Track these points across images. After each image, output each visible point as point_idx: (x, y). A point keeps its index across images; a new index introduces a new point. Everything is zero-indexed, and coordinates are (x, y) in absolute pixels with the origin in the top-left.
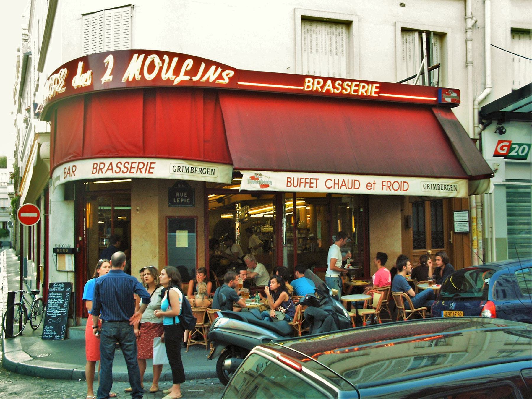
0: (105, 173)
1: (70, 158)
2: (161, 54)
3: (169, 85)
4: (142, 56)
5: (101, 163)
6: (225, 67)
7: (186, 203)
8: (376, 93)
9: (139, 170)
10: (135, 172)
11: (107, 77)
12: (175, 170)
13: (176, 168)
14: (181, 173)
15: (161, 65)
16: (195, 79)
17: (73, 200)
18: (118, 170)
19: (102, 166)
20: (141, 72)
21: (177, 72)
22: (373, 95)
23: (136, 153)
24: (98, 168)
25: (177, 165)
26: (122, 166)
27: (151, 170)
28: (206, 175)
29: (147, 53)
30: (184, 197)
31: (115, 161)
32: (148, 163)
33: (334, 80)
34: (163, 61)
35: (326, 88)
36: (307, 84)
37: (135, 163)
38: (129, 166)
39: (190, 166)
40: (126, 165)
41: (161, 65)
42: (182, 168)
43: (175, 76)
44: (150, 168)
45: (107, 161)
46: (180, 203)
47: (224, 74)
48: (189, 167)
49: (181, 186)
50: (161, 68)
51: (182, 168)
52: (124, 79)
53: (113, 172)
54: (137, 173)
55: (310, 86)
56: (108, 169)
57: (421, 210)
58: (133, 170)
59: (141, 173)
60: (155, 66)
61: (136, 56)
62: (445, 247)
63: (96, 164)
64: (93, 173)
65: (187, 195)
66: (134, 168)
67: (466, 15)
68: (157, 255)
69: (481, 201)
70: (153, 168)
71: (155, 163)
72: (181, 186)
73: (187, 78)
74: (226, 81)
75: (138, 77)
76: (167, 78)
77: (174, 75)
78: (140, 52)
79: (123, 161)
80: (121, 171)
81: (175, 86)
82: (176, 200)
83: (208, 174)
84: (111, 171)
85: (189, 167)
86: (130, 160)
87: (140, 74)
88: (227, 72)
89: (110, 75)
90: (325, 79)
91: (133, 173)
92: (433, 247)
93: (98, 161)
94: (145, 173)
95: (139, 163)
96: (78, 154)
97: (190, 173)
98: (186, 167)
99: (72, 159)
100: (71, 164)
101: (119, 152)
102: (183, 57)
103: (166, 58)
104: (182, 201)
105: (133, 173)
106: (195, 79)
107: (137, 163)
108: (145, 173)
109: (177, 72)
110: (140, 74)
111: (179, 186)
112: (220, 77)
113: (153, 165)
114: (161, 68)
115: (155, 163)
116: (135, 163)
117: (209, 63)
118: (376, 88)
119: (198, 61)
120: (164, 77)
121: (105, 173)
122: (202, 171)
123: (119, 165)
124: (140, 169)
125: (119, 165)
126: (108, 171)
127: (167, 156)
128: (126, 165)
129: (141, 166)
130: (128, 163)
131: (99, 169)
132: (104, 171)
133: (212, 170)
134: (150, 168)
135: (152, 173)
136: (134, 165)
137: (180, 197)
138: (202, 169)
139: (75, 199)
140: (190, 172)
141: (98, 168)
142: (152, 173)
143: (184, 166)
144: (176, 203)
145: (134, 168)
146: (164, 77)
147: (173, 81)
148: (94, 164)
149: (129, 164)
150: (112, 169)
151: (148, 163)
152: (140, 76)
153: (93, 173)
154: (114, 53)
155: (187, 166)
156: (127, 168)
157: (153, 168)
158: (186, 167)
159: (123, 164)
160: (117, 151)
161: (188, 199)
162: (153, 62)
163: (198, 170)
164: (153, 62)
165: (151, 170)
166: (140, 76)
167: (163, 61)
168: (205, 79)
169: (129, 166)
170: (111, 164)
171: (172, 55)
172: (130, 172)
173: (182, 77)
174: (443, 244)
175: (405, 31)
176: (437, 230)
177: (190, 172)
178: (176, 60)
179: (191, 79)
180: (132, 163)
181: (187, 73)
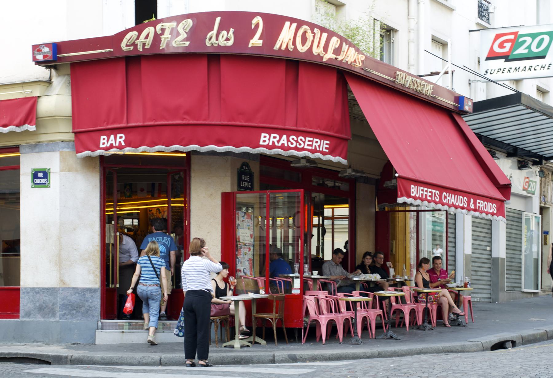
2: (312, 26)
3: (317, 61)
4: (294, 25)
11: (256, 41)
15: (313, 39)
16: (340, 58)
20: (294, 43)
29: (300, 23)
30: (247, 181)
41: (313, 39)
50: (313, 41)
52: (277, 47)
61: (287, 24)
67: (408, 15)
73: (334, 56)
75: (291, 47)
78: (292, 20)
82: (242, 184)
88: (360, 56)
89: (260, 39)
103: (316, 30)
104: (246, 185)
111: (244, 167)
137: (245, 181)
146: (315, 51)
147: (322, 58)
154: (265, 16)
162: (305, 32)
164: (305, 32)
171: (323, 30)
173: (329, 56)
178: (325, 35)
179: (336, 59)
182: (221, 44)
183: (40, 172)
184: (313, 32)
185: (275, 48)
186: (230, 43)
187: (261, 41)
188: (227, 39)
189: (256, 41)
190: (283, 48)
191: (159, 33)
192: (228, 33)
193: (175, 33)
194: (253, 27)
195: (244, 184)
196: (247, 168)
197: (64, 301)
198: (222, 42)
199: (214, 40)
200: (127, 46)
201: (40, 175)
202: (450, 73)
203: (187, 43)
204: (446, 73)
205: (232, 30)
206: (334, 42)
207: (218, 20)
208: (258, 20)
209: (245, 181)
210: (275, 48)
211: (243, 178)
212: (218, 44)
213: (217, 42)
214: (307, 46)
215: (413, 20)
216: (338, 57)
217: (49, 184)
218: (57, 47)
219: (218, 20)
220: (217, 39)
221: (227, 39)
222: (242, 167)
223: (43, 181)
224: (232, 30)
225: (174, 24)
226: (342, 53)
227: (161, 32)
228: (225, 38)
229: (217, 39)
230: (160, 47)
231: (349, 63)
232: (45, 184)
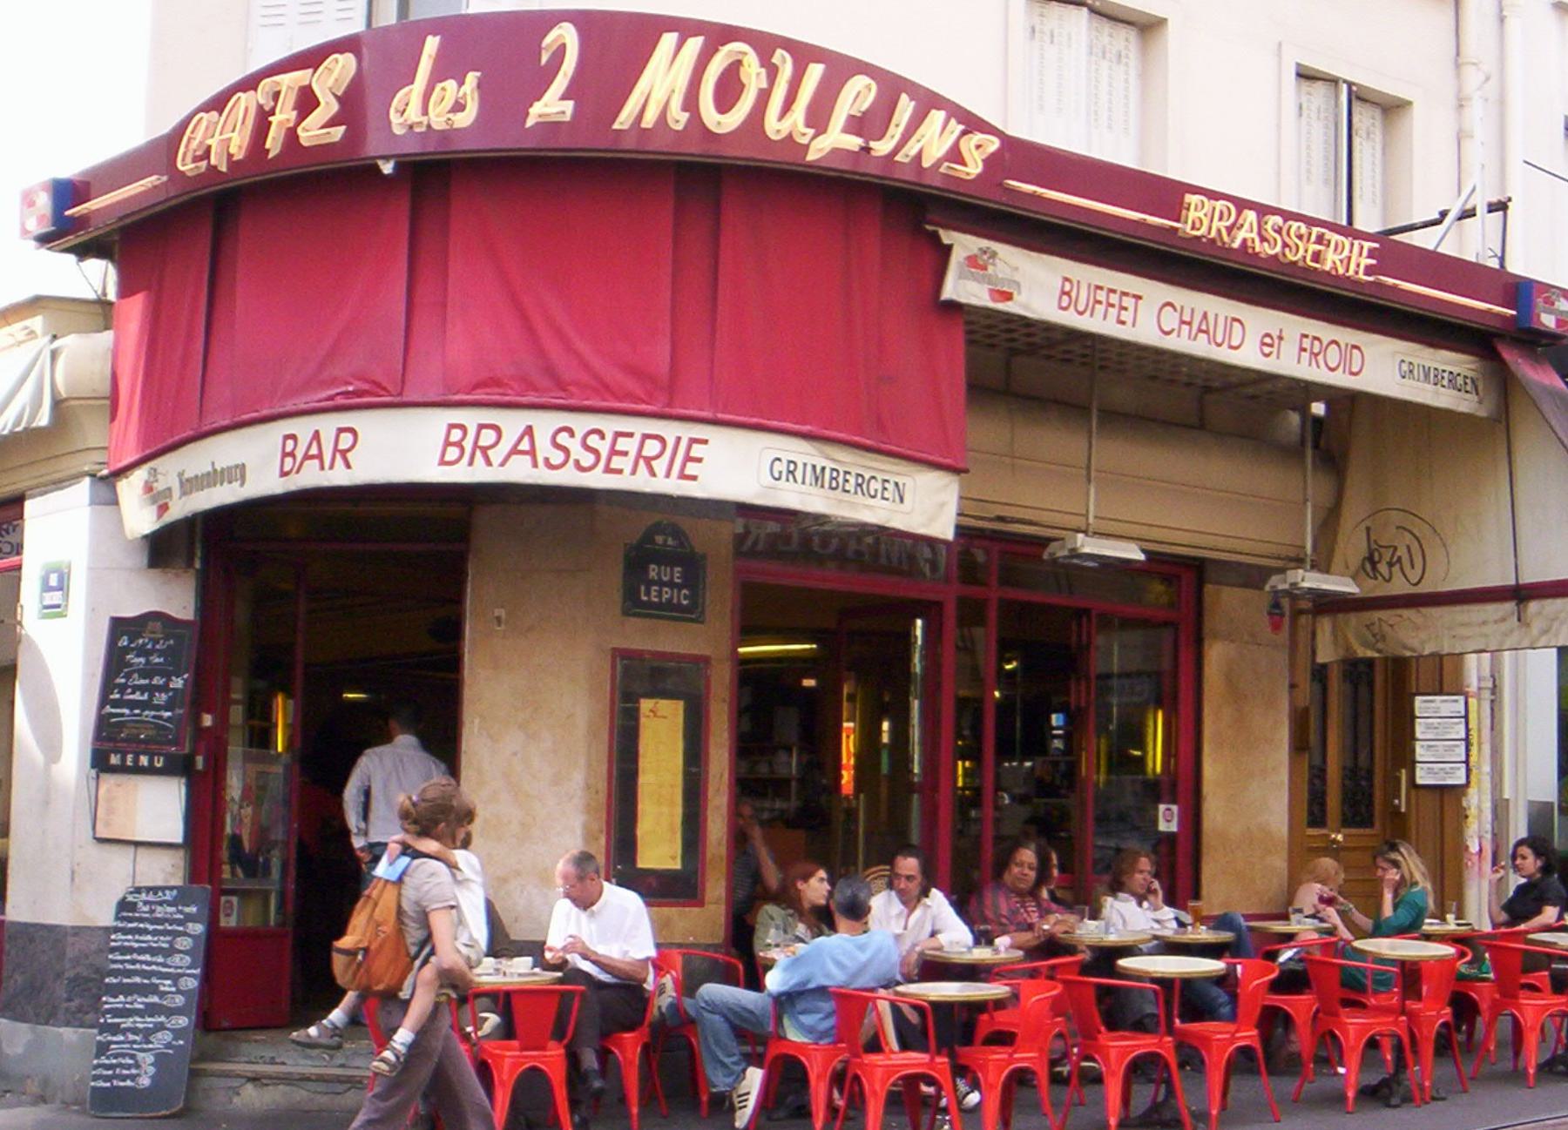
0: (502, 464)
1: (331, 398)
2: (765, 44)
4: (694, 44)
5: (481, 427)
6: (973, 124)
7: (679, 608)
8: (1369, 270)
9: (642, 462)
10: (627, 471)
11: (552, 105)
12: (777, 475)
13: (781, 467)
14: (799, 486)
15: (764, 85)
16: (882, 147)
17: (190, 564)
18: (557, 457)
19: (488, 437)
20: (691, 102)
21: (818, 118)
22: (1362, 276)
25: (785, 457)
26: (574, 445)
27: (691, 469)
28: (878, 502)
29: (719, 35)
30: (671, 584)
31: (545, 423)
32: (679, 439)
33: (1263, 210)
34: (773, 72)
35: (1241, 235)
36: (1192, 215)
37: (630, 435)
38: (603, 447)
39: (829, 465)
40: (593, 441)
41: (764, 85)
42: (800, 467)
43: (811, 132)
44: (688, 458)
45: (512, 423)
46: (659, 606)
47: (969, 145)
48: (823, 469)
49: (665, 541)
50: (764, 97)
51: (800, 467)
52: (624, 120)
53: (535, 465)
54: (634, 472)
55: (1200, 220)
56: (515, 451)
57: (1363, 690)
58: (617, 462)
59: (653, 474)
60: (741, 87)
61: (668, 40)
62: (1377, 823)
63: (463, 428)
64: (443, 462)
65: (684, 576)
66: (625, 454)
67: (1458, 54)
68: (579, 793)
69: (1493, 676)
70: (699, 460)
71: (705, 442)
72: (665, 541)
73: (854, 142)
74: (973, 168)
76: (783, 135)
77: (808, 125)
78: (686, 28)
79: (582, 423)
80: (571, 462)
81: (810, 165)
82: (648, 593)
83: (883, 498)
84: (528, 458)
85: (823, 469)
86: (610, 424)
87: (685, 109)
88: (978, 137)
89: (564, 97)
90: (1242, 204)
91: (620, 471)
92: (1346, 822)
93: (471, 418)
94: (668, 475)
95: (646, 437)
96: (378, 385)
97: (826, 492)
98: (814, 467)
99: (340, 401)
100: (328, 425)
101: (572, 389)
102: (841, 68)
104: (665, 597)
105: (620, 471)
106: (882, 147)
107: (638, 437)
108: (668, 475)
109: (818, 118)
110: (685, 109)
111: (659, 539)
112: (955, 155)
113: (697, 451)
114: (764, 97)
115: (705, 442)
116: (630, 435)
117: (928, 101)
118: (1371, 254)
119: (892, 86)
120: (775, 127)
121: (502, 464)
122: (865, 486)
123: (563, 438)
124: (648, 460)
125: (563, 438)
126: (514, 457)
127: (755, 420)
128: (593, 441)
129: (652, 448)
130: (602, 436)
131: (336, 449)
132: (496, 455)
133: (897, 484)
134: (688, 458)
135: (694, 478)
136: (622, 444)
137: (661, 584)
138: (867, 477)
139: (198, 565)
140: (827, 485)
142: (694, 478)
143: (811, 461)
144: (650, 605)
145: (625, 454)
146: (775, 127)
147: (807, 147)
148: (452, 426)
149: (602, 436)
150: (532, 452)
151: (679, 439)
152: (684, 117)
153: (443, 462)
154: (582, 20)
155: (820, 462)
156: (596, 452)
157: (699, 460)
158: (814, 467)
159: (579, 435)
160: (561, 386)
161: (685, 591)
163: (852, 480)
165: (691, 469)
166: (687, 115)
167: (773, 72)
168: (912, 149)
169: (603, 447)
170: (529, 431)
171: (804, 54)
172: (608, 470)
173: (835, 140)
174: (1372, 816)
175: (1306, 75)
176: (1356, 765)
177: (827, 485)
178: (815, 72)
180: (618, 434)
181: (856, 125)
182: (436, 127)
183: (54, 572)
184: (766, 61)
185: (616, 126)
186: (464, 119)
187: (569, 106)
188: (459, 107)
189: (552, 105)
190: (649, 120)
191: (267, 108)
192: (461, 83)
193: (307, 102)
194: (545, 58)
195: (654, 593)
196: (670, 542)
197: (79, 969)
198: (438, 118)
199: (413, 114)
201: (53, 581)
202: (1481, 210)
203: (338, 132)
204: (1468, 214)
205: (472, 78)
206: (857, 95)
207: (432, 44)
208: (567, 34)
209: (661, 584)
210: (616, 126)
211: (653, 574)
212: (429, 126)
213: (425, 120)
214: (893, 137)
215: (1474, 67)
216: (872, 144)
217: (66, 606)
218: (68, 193)
219: (432, 44)
220: (425, 112)
221: (459, 107)
222: (648, 536)
223: (55, 597)
224: (472, 78)
225: (300, 77)
226: (892, 129)
227: (272, 104)
228: (449, 102)
229: (425, 112)
230: (268, 151)
231: (926, 164)
232: (58, 606)
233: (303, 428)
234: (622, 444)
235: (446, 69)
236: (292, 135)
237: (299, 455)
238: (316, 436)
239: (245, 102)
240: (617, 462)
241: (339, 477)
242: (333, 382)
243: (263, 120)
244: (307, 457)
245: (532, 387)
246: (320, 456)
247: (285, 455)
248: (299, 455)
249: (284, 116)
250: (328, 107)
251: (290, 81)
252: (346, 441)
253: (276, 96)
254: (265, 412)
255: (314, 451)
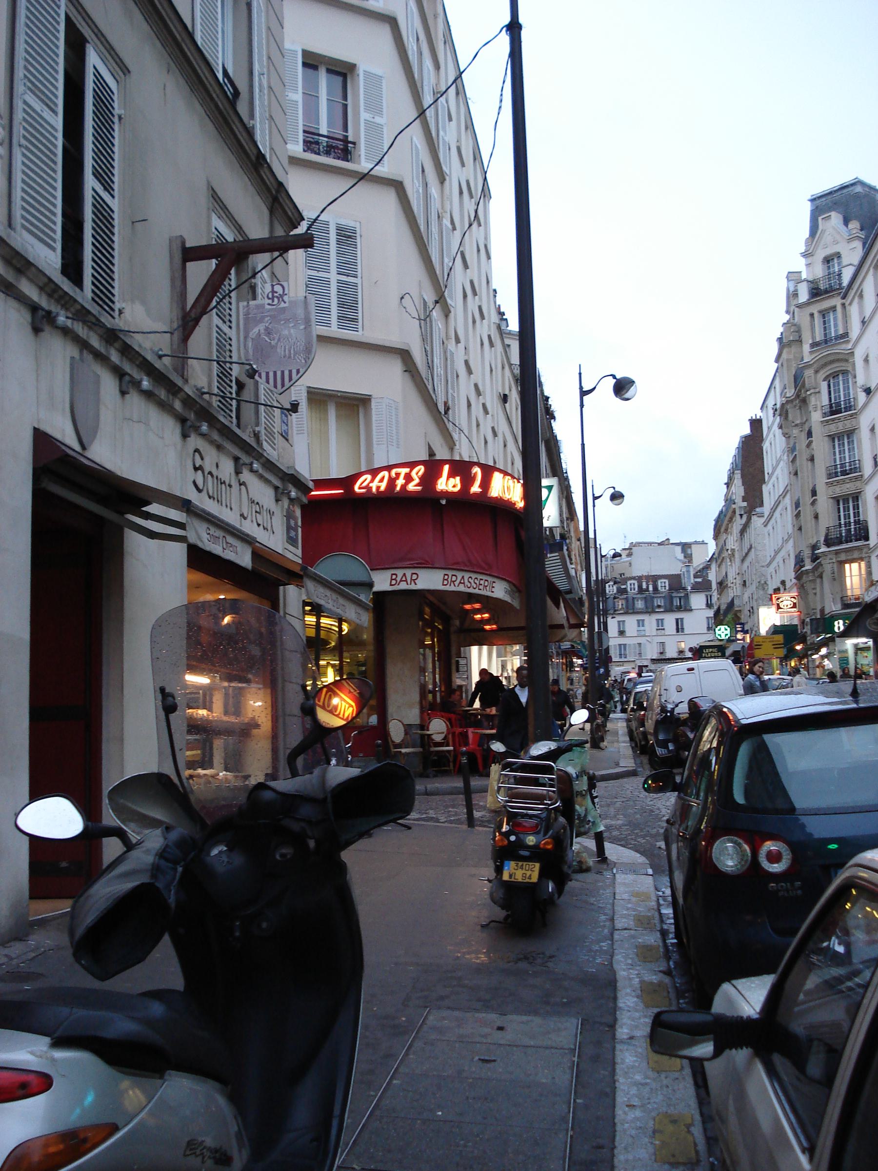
5: (453, 575)
11: (476, 488)
23: (486, 570)
24: (449, 580)
26: (472, 581)
27: (493, 590)
31: (467, 575)
38: (477, 582)
40: (476, 581)
45: (460, 575)
56: (460, 583)
58: (481, 587)
79: (474, 576)
86: (480, 577)
93: (450, 573)
96: (427, 562)
100: (409, 573)
128: (476, 581)
132: (457, 583)
141: (449, 580)
150: (464, 583)
159: (473, 578)
165: (493, 590)
188: (454, 486)
193: (408, 478)
198: (450, 489)
200: (360, 488)
207: (446, 468)
225: (407, 470)
233: (400, 573)
234: (482, 582)
235: (451, 475)
236: (404, 487)
237: (398, 579)
238: (404, 575)
239: (385, 474)
240: (481, 587)
241: (413, 587)
242: (412, 559)
243: (392, 482)
244: (401, 581)
245: (466, 565)
246: (406, 581)
247: (392, 579)
248: (398, 579)
249: (400, 482)
250: (417, 481)
251: (404, 471)
252: (414, 577)
253: (398, 475)
254: (387, 566)
255: (404, 579)
